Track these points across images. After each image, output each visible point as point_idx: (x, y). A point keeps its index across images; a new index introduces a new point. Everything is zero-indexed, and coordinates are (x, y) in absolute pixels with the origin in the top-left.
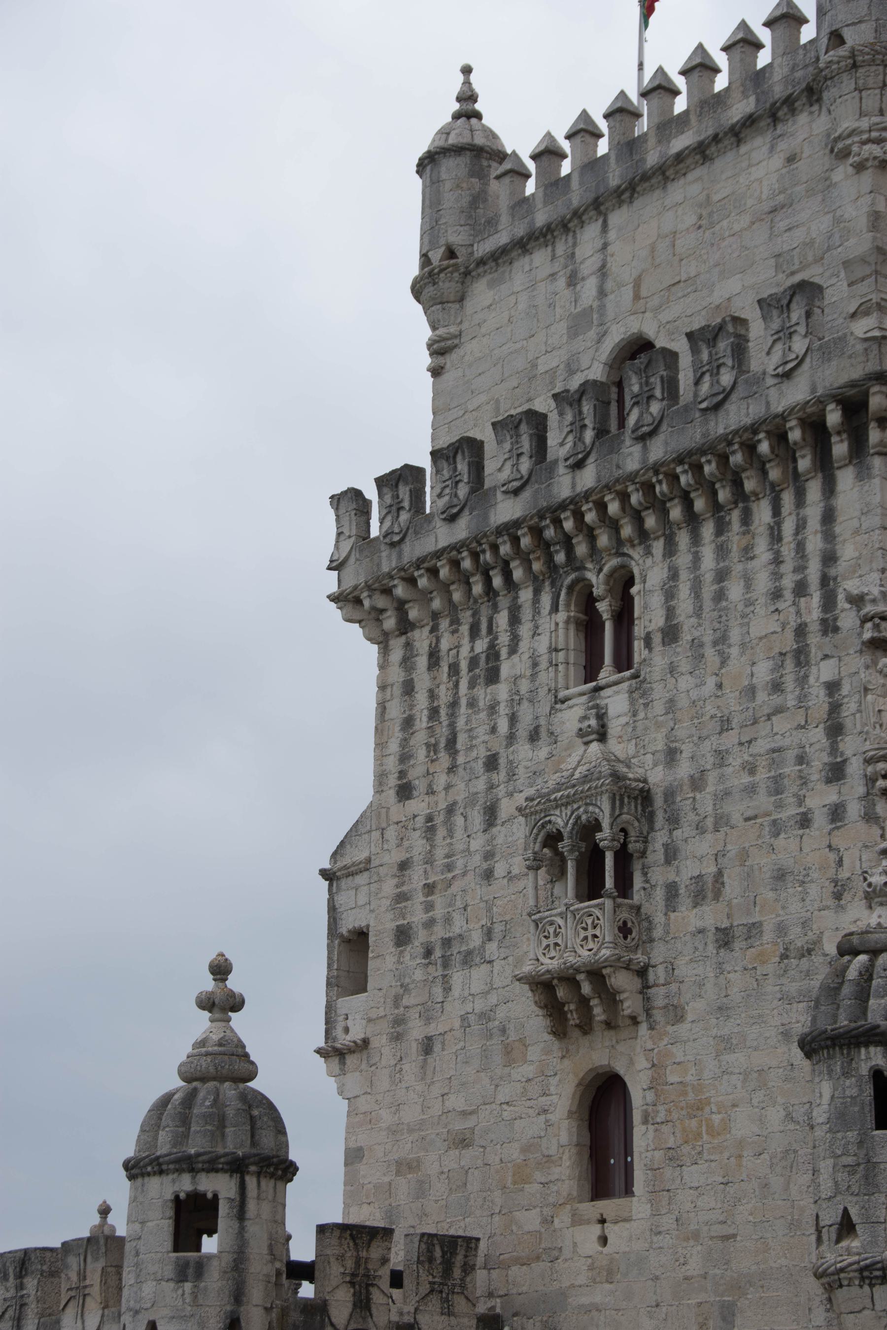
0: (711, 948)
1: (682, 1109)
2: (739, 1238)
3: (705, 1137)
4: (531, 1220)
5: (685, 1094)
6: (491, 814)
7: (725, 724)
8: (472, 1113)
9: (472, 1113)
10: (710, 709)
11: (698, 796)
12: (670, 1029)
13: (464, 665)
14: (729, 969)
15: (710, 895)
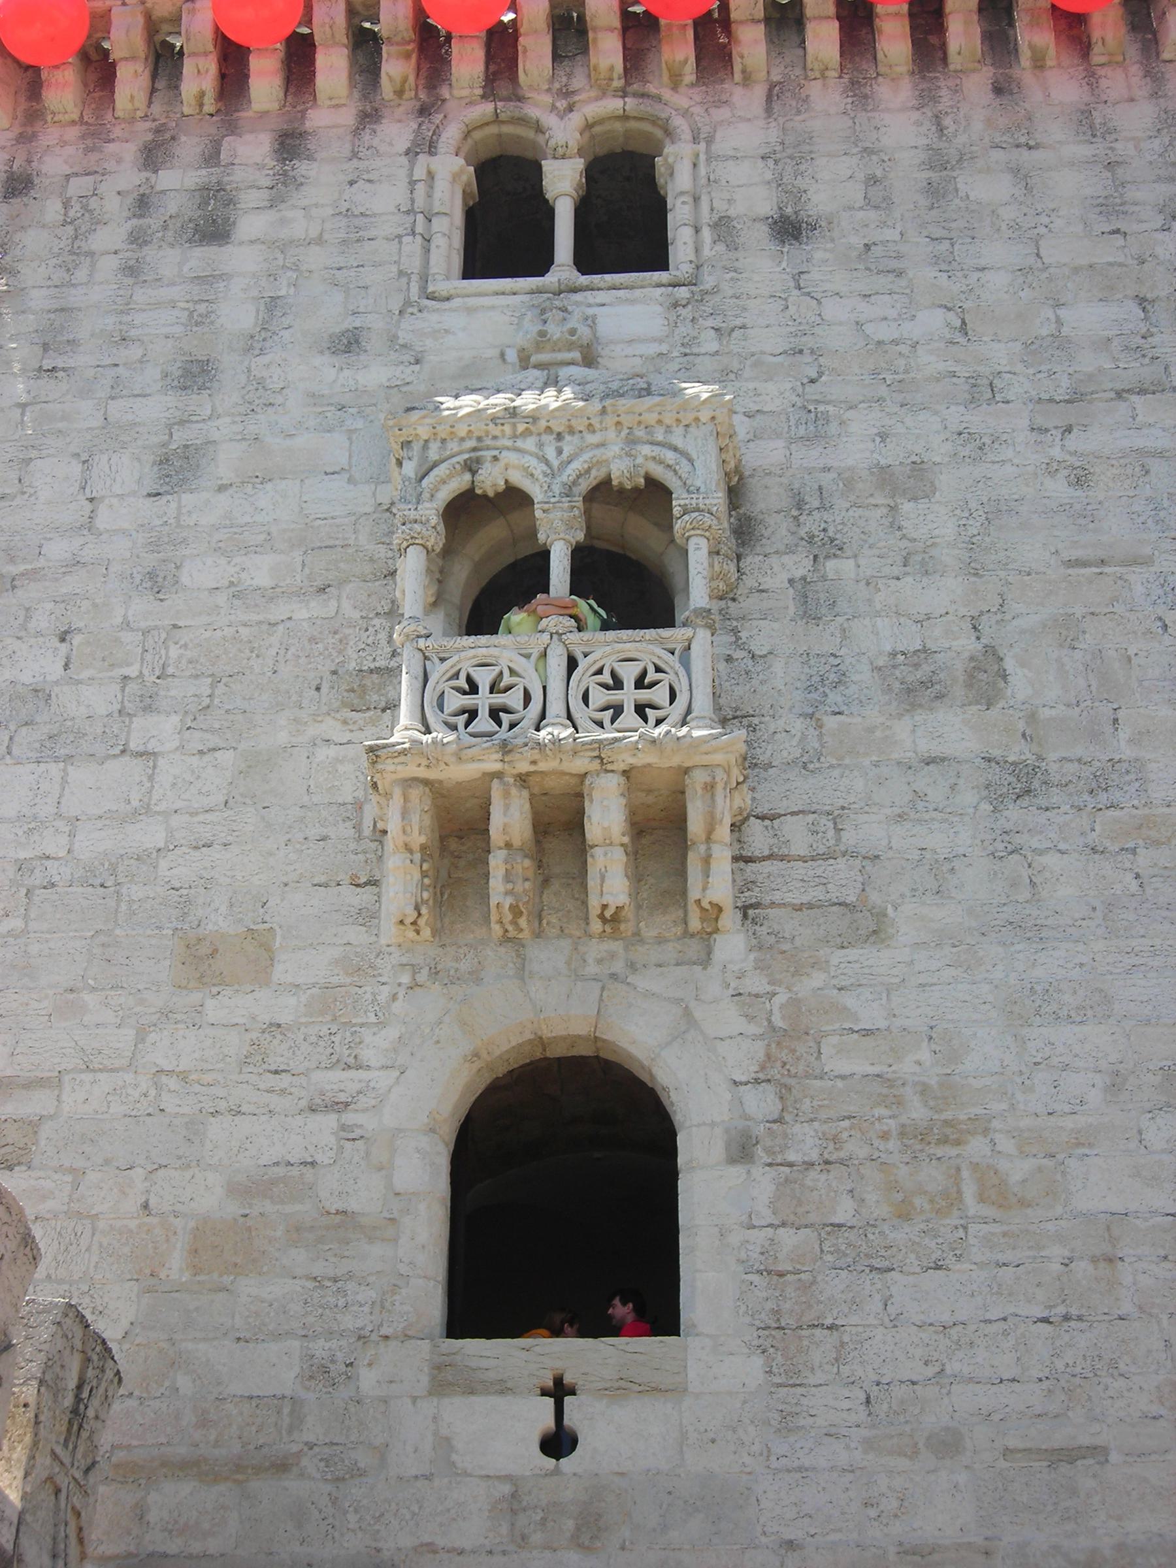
0: (968, 797)
1: (885, 1136)
2: (1114, 1457)
3: (973, 1207)
4: (277, 1369)
5: (899, 1102)
6: (176, 468)
7: (984, 390)
8: (30, 1085)
9: (30, 1085)
10: (929, 362)
11: (907, 507)
12: (837, 956)
13: (113, 206)
14: (1035, 844)
15: (959, 691)
